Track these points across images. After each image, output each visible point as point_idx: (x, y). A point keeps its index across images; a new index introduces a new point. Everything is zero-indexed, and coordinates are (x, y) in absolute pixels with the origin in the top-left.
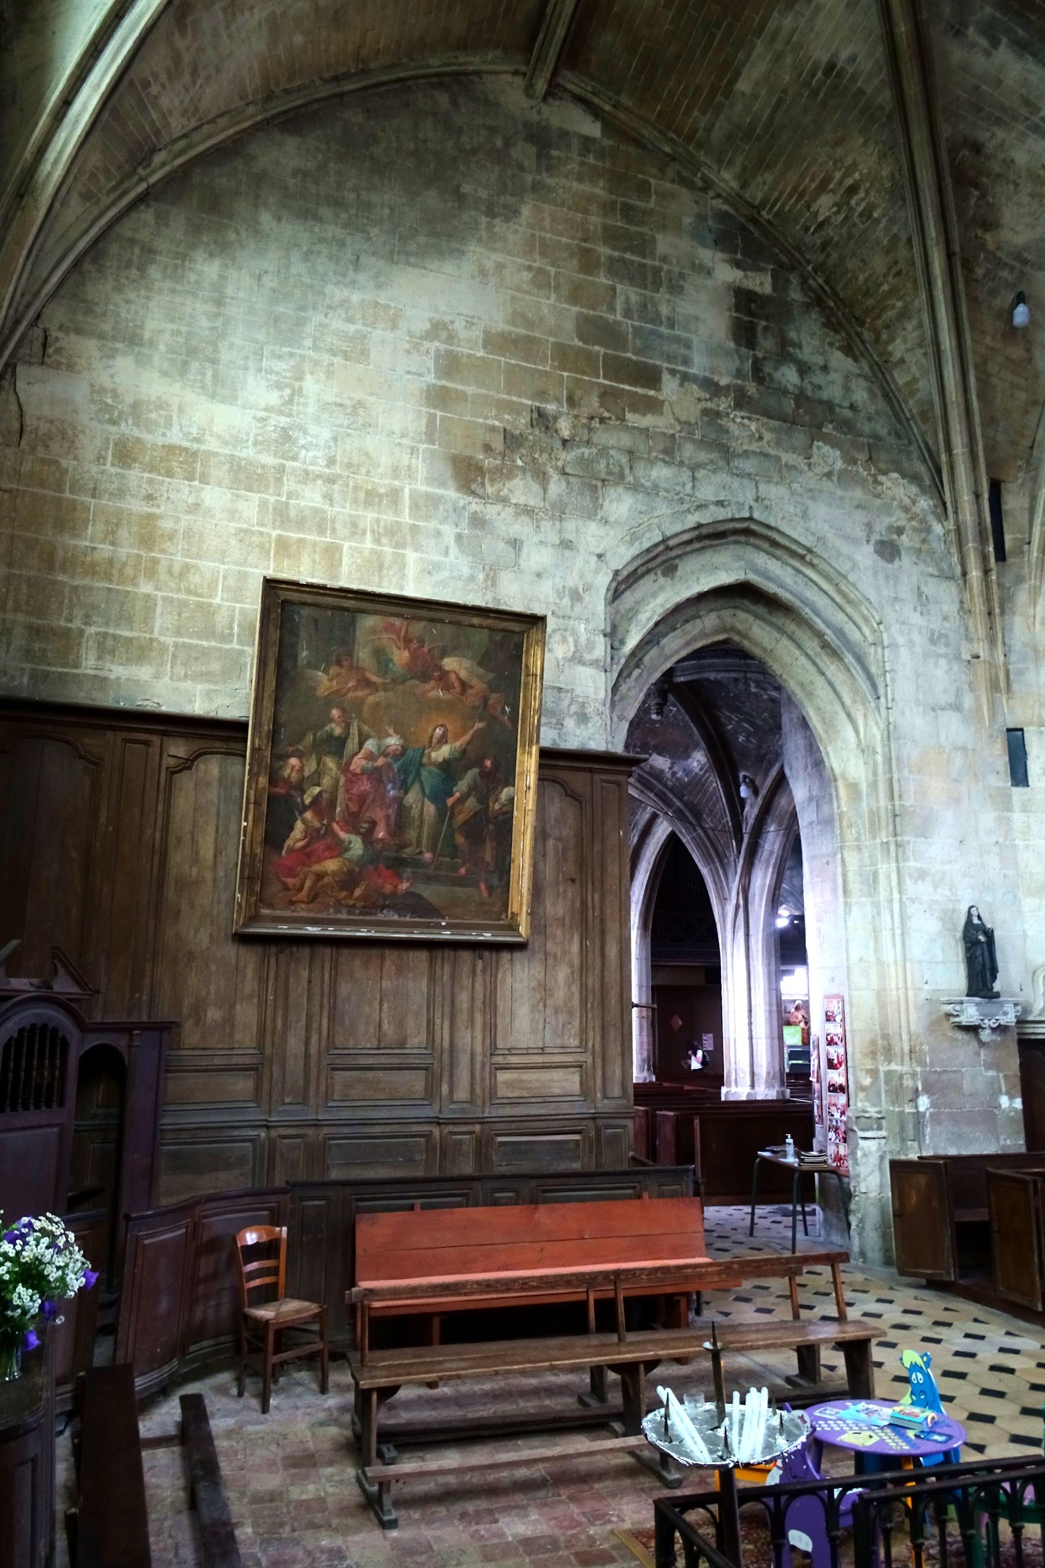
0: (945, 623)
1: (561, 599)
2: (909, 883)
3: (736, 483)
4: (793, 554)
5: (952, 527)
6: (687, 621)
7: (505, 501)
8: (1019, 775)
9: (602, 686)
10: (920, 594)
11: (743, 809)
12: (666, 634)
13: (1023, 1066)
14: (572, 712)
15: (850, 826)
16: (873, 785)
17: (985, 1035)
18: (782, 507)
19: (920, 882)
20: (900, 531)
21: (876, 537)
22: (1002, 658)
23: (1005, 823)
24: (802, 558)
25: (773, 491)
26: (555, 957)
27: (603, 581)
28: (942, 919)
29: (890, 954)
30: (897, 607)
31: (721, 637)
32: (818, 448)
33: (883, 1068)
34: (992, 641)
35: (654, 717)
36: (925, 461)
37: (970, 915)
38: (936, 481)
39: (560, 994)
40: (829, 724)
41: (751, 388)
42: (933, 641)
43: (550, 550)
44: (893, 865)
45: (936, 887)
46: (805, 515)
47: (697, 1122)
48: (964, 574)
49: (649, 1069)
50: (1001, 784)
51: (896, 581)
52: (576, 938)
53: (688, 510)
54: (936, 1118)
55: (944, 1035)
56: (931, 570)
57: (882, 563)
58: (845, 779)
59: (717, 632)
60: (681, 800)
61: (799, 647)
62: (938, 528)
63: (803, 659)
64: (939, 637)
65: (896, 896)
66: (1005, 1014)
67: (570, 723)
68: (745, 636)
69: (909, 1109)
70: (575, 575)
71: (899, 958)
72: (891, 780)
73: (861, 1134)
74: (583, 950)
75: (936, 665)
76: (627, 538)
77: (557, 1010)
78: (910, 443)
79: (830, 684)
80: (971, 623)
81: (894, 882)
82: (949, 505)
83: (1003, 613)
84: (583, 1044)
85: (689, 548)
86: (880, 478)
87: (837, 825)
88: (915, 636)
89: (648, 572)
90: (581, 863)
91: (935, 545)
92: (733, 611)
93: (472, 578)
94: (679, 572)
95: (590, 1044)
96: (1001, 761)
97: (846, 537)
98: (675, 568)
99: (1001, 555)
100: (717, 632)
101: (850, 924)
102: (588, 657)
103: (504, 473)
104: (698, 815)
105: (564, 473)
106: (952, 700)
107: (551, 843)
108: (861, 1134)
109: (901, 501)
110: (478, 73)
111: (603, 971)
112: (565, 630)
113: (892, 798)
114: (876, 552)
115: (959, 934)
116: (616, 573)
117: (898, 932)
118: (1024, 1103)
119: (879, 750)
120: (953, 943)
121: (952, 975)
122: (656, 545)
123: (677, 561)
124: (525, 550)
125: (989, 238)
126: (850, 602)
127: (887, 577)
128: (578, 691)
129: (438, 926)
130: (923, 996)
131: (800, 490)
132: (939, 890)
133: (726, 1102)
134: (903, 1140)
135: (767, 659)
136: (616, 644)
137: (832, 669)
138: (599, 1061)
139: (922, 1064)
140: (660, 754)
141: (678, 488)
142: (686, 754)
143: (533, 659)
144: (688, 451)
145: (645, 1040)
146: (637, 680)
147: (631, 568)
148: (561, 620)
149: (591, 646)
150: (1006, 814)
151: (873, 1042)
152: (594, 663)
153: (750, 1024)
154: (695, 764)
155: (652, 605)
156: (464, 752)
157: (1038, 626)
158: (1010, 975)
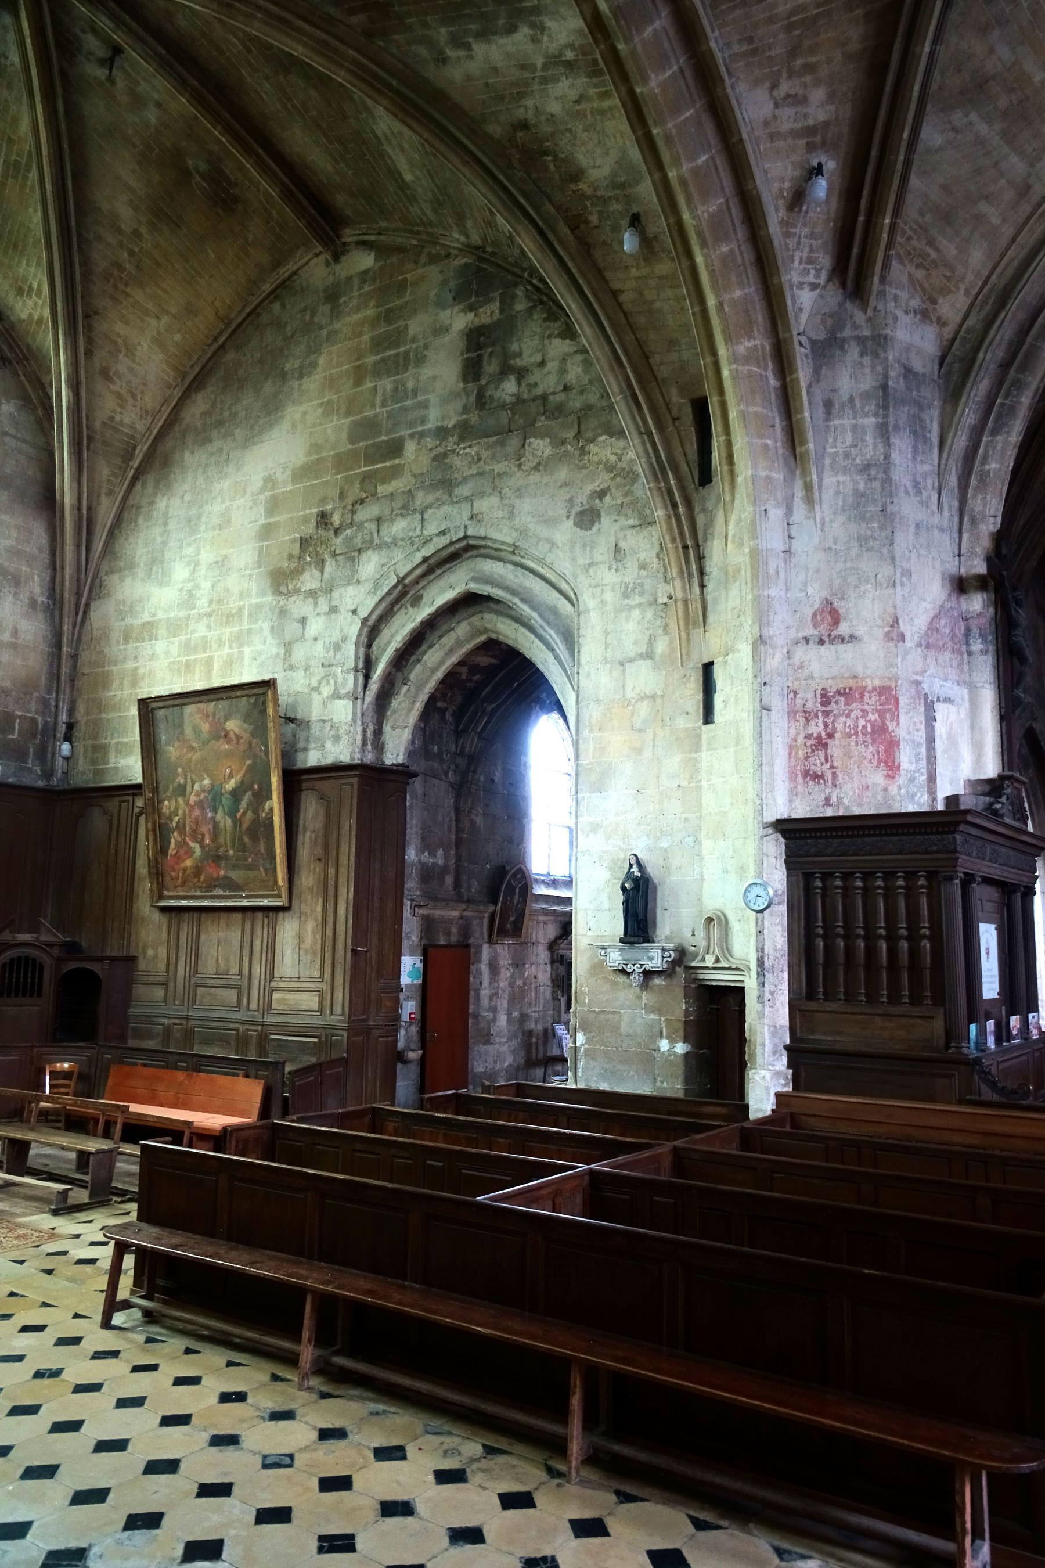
0: (643, 573)
6: (441, 637)
7: (297, 591)
19: (591, 835)
20: (601, 494)
23: (692, 767)
25: (486, 505)
27: (353, 629)
28: (611, 869)
30: (591, 571)
39: (309, 940)
41: (474, 418)
42: (626, 595)
43: (323, 617)
45: (608, 838)
46: (511, 515)
51: (593, 545)
52: (320, 900)
56: (631, 522)
59: (473, 636)
63: (537, 641)
66: (651, 959)
67: (329, 744)
68: (496, 632)
70: (338, 632)
75: (627, 619)
77: (306, 951)
84: (322, 976)
85: (432, 577)
88: (608, 596)
90: (326, 848)
93: (278, 654)
98: (421, 597)
100: (473, 636)
103: (298, 572)
105: (334, 555)
107: (308, 834)
110: (295, 273)
122: (395, 587)
125: (582, 186)
127: (584, 546)
128: (335, 720)
129: (241, 897)
132: (611, 841)
144: (421, 498)
150: (694, 755)
152: (346, 696)
156: (242, 782)
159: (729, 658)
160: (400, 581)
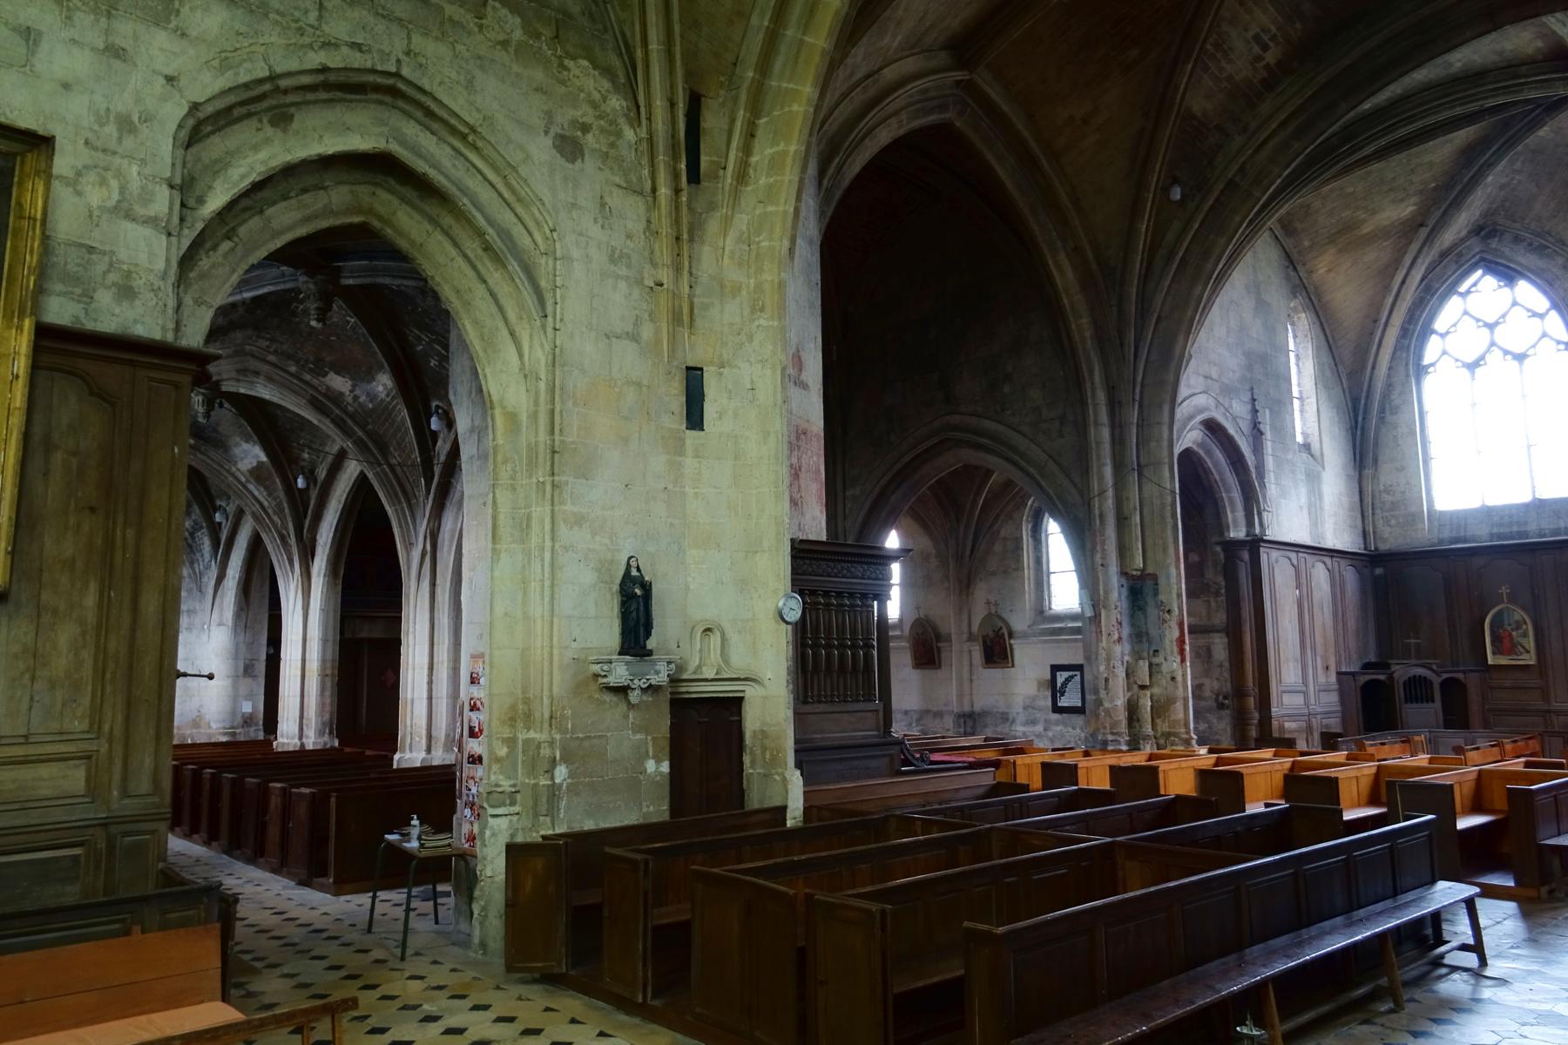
1: (102, 125)
2: (563, 530)
3: (381, 27)
4: (453, 131)
5: (644, 135)
6: (305, 191)
8: (694, 418)
9: (162, 254)
10: (603, 205)
11: (435, 443)
12: (274, 203)
13: (673, 727)
14: (109, 281)
15: (505, 462)
16: (534, 416)
17: (634, 696)
18: (438, 67)
20: (586, 128)
21: (555, 130)
22: (687, 289)
24: (464, 137)
26: (55, 612)
27: (173, 112)
28: (598, 570)
29: (538, 609)
30: (574, 214)
31: (356, 219)
32: (494, 8)
33: (522, 736)
34: (678, 269)
35: (313, 323)
36: (621, 54)
37: (629, 565)
38: (630, 82)
39: (61, 664)
40: (489, 342)
44: (548, 509)
45: (594, 534)
46: (470, 85)
47: (333, 800)
48: (654, 190)
49: (331, 733)
50: (674, 426)
52: (93, 586)
53: (311, 46)
54: (573, 790)
55: (590, 697)
56: (617, 180)
57: (560, 161)
58: (504, 408)
59: (350, 211)
60: (363, 428)
61: (456, 245)
62: (629, 134)
63: (460, 261)
64: (621, 257)
65: (548, 543)
66: (657, 673)
67: (104, 298)
68: (388, 223)
69: (544, 781)
71: (547, 614)
72: (552, 412)
73: (491, 811)
74: (104, 605)
75: (615, 288)
76: (216, 63)
77: (52, 685)
78: (606, 31)
79: (492, 294)
80: (657, 247)
81: (548, 527)
82: (643, 109)
83: (691, 240)
85: (310, 96)
86: (566, 62)
87: (491, 460)
89: (249, 115)
91: (624, 153)
92: (373, 189)
94: (295, 125)
95: (106, 727)
96: (678, 402)
97: (519, 122)
98: (289, 118)
99: (694, 176)
101: (497, 574)
102: (140, 211)
104: (383, 448)
106: (630, 328)
107: (58, 457)
108: (491, 811)
109: (589, 94)
111: (133, 630)
112: (106, 169)
113: (552, 432)
114: (555, 146)
115: (616, 587)
116: (195, 107)
117: (547, 583)
118: (671, 767)
119: (543, 376)
120: (608, 596)
121: (609, 634)
122: (261, 81)
123: (293, 110)
124: (45, 46)
126: (520, 200)
127: (565, 179)
128: (123, 254)
130: (570, 654)
131: (467, 55)
132: (597, 538)
133: (398, 770)
134: (536, 815)
135: (416, 254)
136: (191, 202)
137: (495, 277)
138: (118, 749)
139: (563, 731)
140: (338, 373)
141: (297, 14)
142: (369, 376)
143: (31, 196)
145: (328, 701)
146: (226, 256)
147: (220, 104)
148: (100, 155)
149: (146, 198)
151: (513, 707)
152: (152, 221)
153: (430, 682)
154: (381, 388)
155: (249, 160)
157: (726, 260)
158: (666, 632)
159: (726, 371)
160: (272, 78)
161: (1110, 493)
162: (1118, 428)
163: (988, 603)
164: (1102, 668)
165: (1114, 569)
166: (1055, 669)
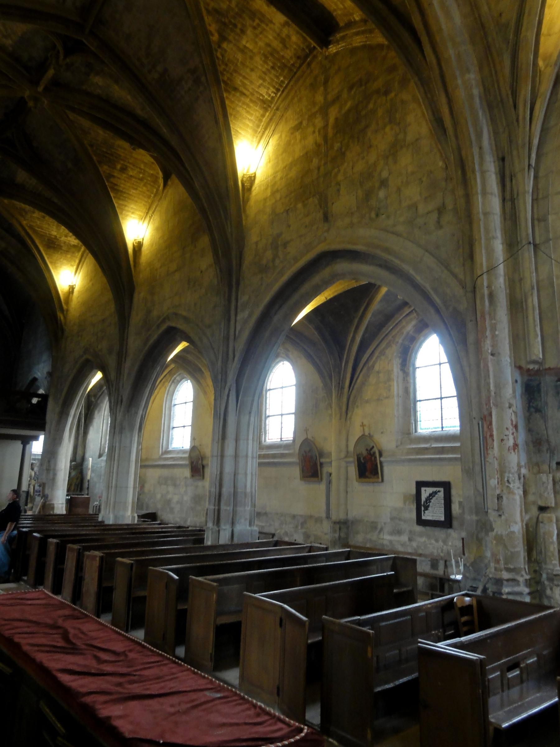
161: (501, 269)
162: (510, 200)
163: (363, 425)
164: (493, 482)
165: (506, 359)
166: (420, 485)
